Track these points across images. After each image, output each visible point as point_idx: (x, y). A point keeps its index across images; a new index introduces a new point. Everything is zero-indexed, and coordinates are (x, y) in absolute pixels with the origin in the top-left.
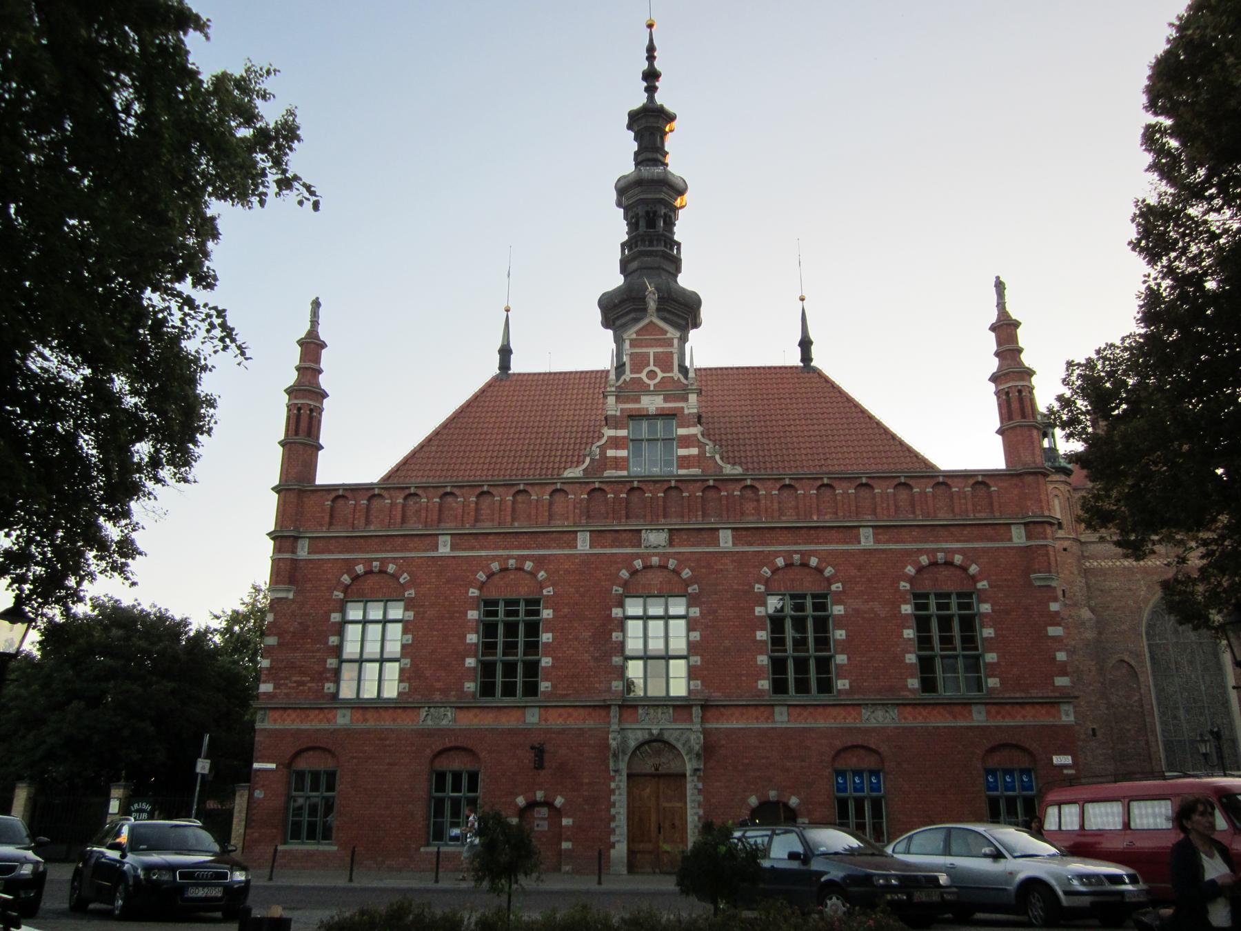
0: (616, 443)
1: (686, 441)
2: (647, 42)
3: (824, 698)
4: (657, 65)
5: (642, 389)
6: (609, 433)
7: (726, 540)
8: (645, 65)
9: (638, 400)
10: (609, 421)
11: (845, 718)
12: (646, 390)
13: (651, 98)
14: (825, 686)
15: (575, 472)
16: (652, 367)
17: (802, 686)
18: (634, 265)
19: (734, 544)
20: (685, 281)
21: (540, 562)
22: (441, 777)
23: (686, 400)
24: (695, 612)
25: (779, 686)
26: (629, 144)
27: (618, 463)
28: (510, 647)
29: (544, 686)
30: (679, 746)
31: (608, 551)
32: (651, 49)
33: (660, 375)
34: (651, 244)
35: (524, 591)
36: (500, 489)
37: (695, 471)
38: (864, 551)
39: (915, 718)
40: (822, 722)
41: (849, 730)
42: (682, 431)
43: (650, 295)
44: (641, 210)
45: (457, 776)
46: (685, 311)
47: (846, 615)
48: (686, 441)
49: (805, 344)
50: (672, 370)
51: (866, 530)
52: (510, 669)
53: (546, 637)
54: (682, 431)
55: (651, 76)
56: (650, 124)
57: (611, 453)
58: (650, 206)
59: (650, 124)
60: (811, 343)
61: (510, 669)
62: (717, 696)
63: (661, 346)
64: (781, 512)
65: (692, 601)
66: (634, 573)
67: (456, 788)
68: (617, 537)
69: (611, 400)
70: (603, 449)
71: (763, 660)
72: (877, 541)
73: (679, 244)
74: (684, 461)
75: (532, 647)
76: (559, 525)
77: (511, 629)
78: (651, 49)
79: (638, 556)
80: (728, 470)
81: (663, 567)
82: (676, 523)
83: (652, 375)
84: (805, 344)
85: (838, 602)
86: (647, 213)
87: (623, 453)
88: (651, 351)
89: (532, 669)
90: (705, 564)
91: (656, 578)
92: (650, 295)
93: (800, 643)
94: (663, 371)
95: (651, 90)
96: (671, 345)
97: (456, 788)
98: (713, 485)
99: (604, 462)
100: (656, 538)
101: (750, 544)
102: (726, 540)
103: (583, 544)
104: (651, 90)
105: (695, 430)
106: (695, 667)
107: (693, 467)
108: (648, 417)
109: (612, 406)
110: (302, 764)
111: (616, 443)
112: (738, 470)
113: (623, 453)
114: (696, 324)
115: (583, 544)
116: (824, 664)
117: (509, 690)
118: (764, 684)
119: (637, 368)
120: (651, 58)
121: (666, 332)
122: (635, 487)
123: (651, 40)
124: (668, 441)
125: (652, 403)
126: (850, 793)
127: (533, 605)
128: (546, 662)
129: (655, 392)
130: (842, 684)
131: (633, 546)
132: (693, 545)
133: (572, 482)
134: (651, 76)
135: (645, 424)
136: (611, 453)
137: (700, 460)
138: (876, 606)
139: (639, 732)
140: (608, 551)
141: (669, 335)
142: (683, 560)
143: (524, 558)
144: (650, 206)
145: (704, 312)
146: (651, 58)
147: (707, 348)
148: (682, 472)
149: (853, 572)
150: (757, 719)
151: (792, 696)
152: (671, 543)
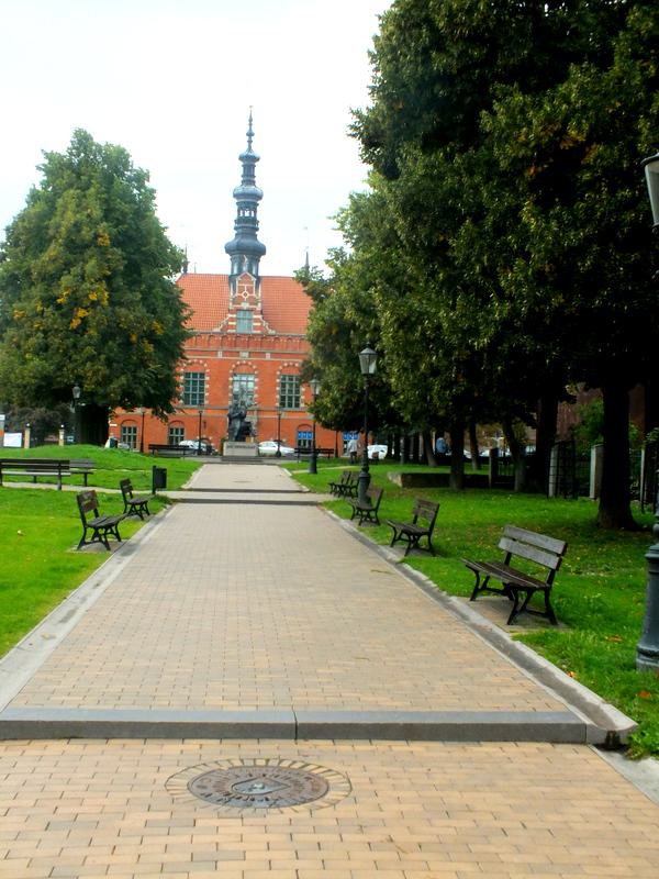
0: (232, 319)
1: (257, 320)
3: (297, 409)
4: (254, 130)
5: (243, 300)
6: (230, 316)
7: (268, 357)
8: (247, 129)
10: (230, 311)
12: (243, 300)
14: (297, 405)
15: (217, 330)
17: (290, 405)
21: (205, 361)
22: (172, 430)
24: (256, 380)
25: (283, 404)
26: (238, 169)
27: (232, 327)
28: (194, 389)
29: (206, 402)
32: (251, 120)
35: (199, 371)
37: (259, 332)
40: (297, 416)
41: (304, 420)
42: (255, 317)
43: (247, 250)
45: (177, 430)
48: (257, 320)
52: (194, 396)
53: (207, 386)
54: (255, 317)
55: (250, 134)
56: (249, 162)
57: (230, 323)
58: (248, 200)
59: (249, 162)
61: (194, 396)
62: (262, 408)
64: (287, 347)
65: (257, 376)
66: (237, 366)
67: (177, 433)
68: (231, 354)
70: (227, 321)
71: (278, 397)
74: (255, 328)
75: (202, 389)
76: (212, 348)
77: (195, 382)
78: (251, 120)
80: (271, 332)
81: (246, 364)
82: (251, 349)
83: (245, 295)
87: (234, 323)
89: (202, 396)
90: (260, 364)
91: (244, 369)
92: (247, 250)
93: (290, 391)
95: (250, 142)
97: (177, 433)
98: (265, 337)
99: (227, 327)
100: (245, 355)
102: (268, 357)
103: (220, 355)
104: (250, 142)
105: (260, 317)
109: (231, 306)
110: (124, 425)
111: (232, 319)
112: (273, 332)
113: (234, 323)
115: (220, 355)
116: (297, 399)
117: (194, 403)
118: (278, 404)
120: (251, 125)
122: (238, 336)
124: (250, 319)
125: (245, 305)
126: (302, 438)
127: (202, 375)
128: (207, 394)
133: (217, 333)
134: (250, 134)
135: (242, 313)
136: (230, 323)
137: (261, 328)
142: (253, 362)
144: (248, 200)
146: (251, 125)
147: (266, 267)
148: (254, 332)
151: (286, 408)
152: (250, 356)
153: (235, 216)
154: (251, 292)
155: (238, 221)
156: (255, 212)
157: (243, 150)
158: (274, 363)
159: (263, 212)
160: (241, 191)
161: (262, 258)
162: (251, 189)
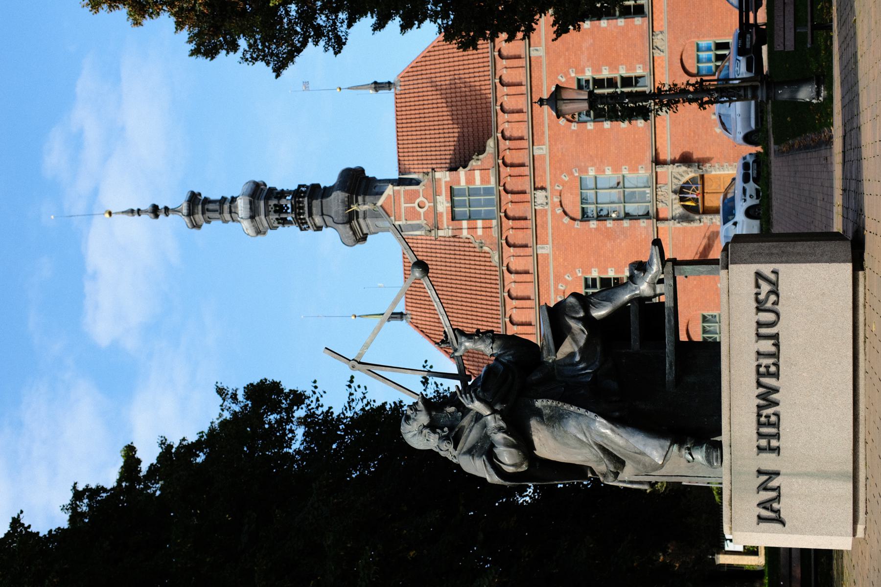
2: (125, 217)
4: (146, 206)
8: (146, 218)
9: (442, 214)
11: (662, 67)
13: (175, 211)
16: (416, 205)
18: (318, 220)
19: (544, 145)
20: (329, 179)
23: (440, 179)
26: (214, 229)
30: (684, 180)
31: (550, 231)
33: (421, 199)
34: (302, 208)
36: (507, 309)
38: (547, 53)
39: (661, 20)
41: (670, 64)
44: (273, 217)
46: (356, 183)
47: (592, 67)
49: (378, 86)
50: (418, 191)
51: (532, 52)
55: (155, 211)
60: (375, 83)
62: (649, 155)
63: (399, 199)
69: (441, 233)
72: (539, 44)
73: (300, 186)
78: (132, 211)
79: (553, 211)
84: (378, 86)
85: (583, 72)
86: (275, 212)
88: (403, 205)
94: (419, 197)
96: (399, 191)
101: (543, 133)
104: (167, 209)
106: (629, 170)
107: (488, 174)
108: (453, 207)
114: (361, 171)
119: (417, 216)
120: (139, 212)
121: (389, 196)
123: (123, 212)
129: (435, 202)
130: (639, 72)
131: (546, 214)
132: (545, 172)
134: (155, 211)
138: (585, 45)
139: (674, 206)
140: (550, 231)
141: (391, 193)
143: (556, 289)
145: (353, 166)
147: (381, 165)
149: (562, 61)
150: (664, 127)
152: (543, 188)
153: (294, 229)
154: (416, 194)
155: (302, 225)
156: (282, 194)
157: (179, 221)
158: (553, 139)
159: (284, 180)
160: (246, 224)
161: (369, 173)
162: (242, 206)
